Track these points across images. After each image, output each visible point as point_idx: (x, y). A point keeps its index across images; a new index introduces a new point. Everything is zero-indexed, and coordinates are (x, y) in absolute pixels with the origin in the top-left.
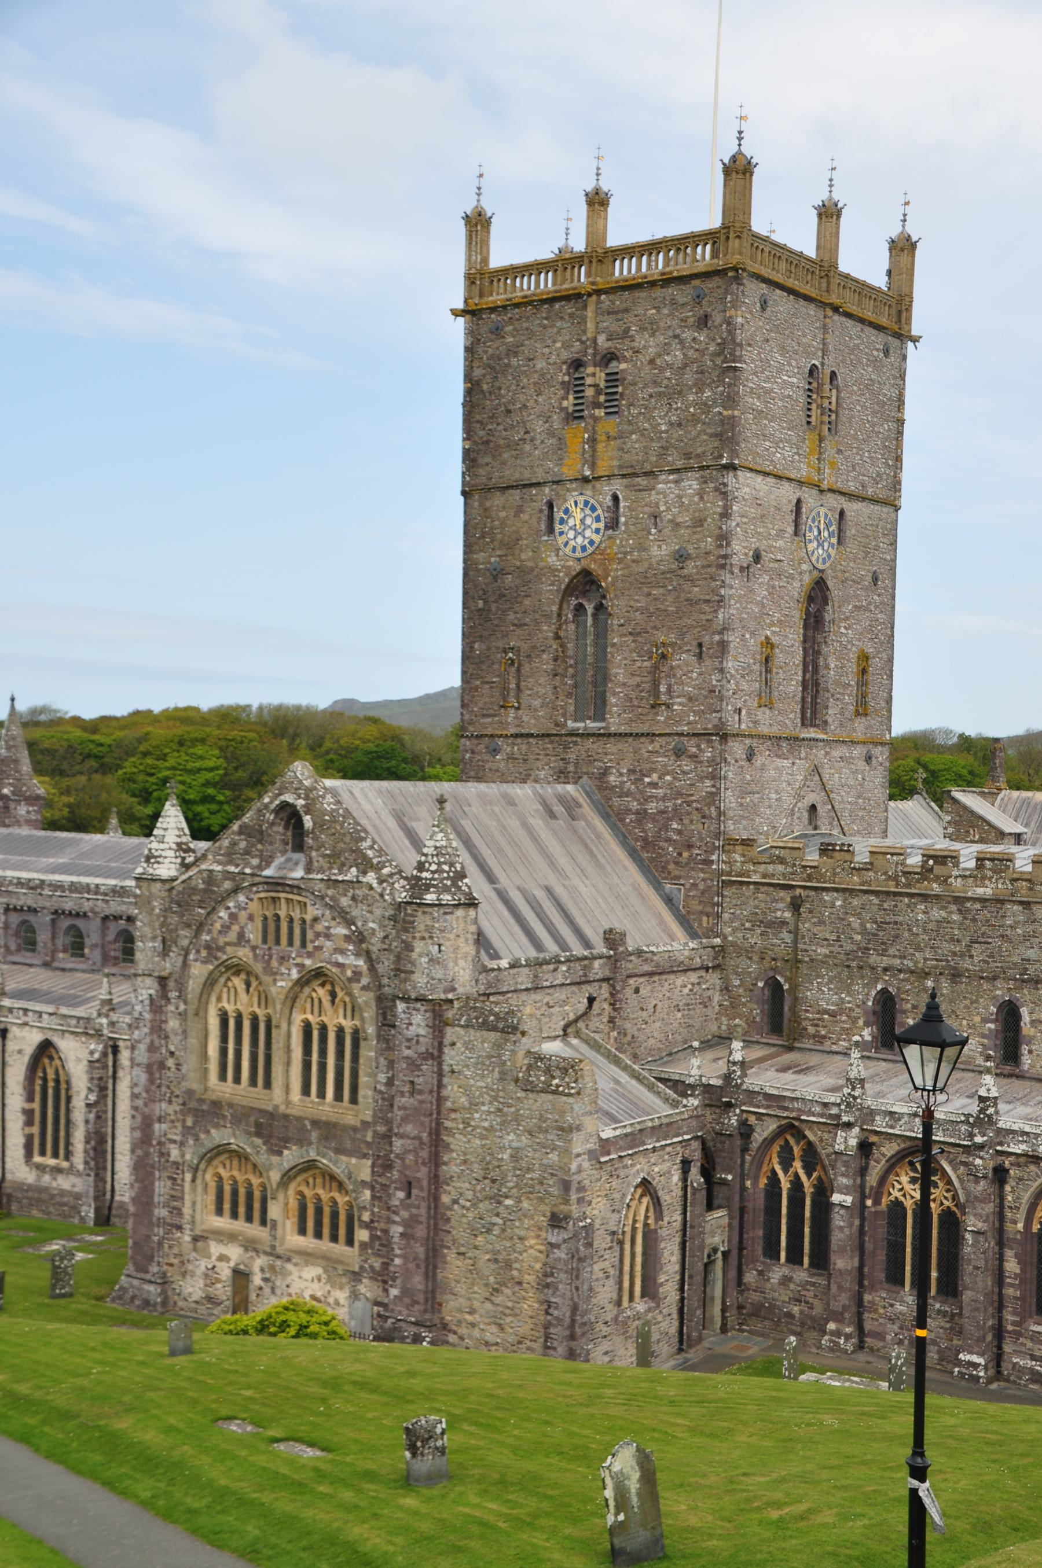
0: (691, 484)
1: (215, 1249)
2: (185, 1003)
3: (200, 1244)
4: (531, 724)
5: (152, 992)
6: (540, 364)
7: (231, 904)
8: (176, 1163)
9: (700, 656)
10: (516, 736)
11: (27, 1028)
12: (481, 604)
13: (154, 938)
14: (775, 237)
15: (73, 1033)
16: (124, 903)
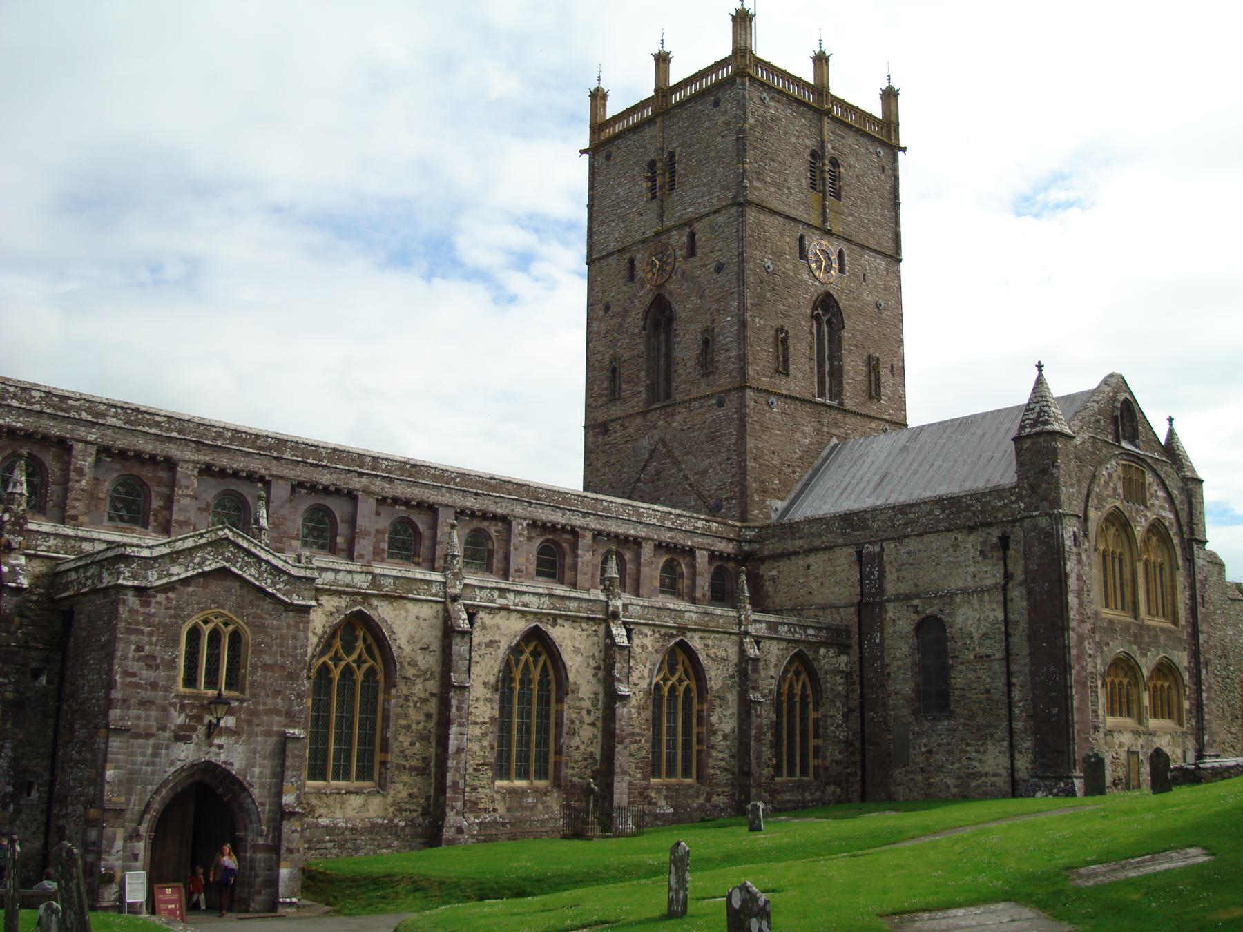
0: (882, 263)
1: (1118, 738)
2: (1089, 541)
3: (1108, 737)
4: (795, 390)
5: (1075, 529)
6: (793, 140)
7: (1109, 466)
8: (1092, 673)
9: (892, 371)
10: (786, 397)
11: (503, 613)
12: (759, 290)
13: (1072, 486)
15: (567, 618)
16: (417, 484)
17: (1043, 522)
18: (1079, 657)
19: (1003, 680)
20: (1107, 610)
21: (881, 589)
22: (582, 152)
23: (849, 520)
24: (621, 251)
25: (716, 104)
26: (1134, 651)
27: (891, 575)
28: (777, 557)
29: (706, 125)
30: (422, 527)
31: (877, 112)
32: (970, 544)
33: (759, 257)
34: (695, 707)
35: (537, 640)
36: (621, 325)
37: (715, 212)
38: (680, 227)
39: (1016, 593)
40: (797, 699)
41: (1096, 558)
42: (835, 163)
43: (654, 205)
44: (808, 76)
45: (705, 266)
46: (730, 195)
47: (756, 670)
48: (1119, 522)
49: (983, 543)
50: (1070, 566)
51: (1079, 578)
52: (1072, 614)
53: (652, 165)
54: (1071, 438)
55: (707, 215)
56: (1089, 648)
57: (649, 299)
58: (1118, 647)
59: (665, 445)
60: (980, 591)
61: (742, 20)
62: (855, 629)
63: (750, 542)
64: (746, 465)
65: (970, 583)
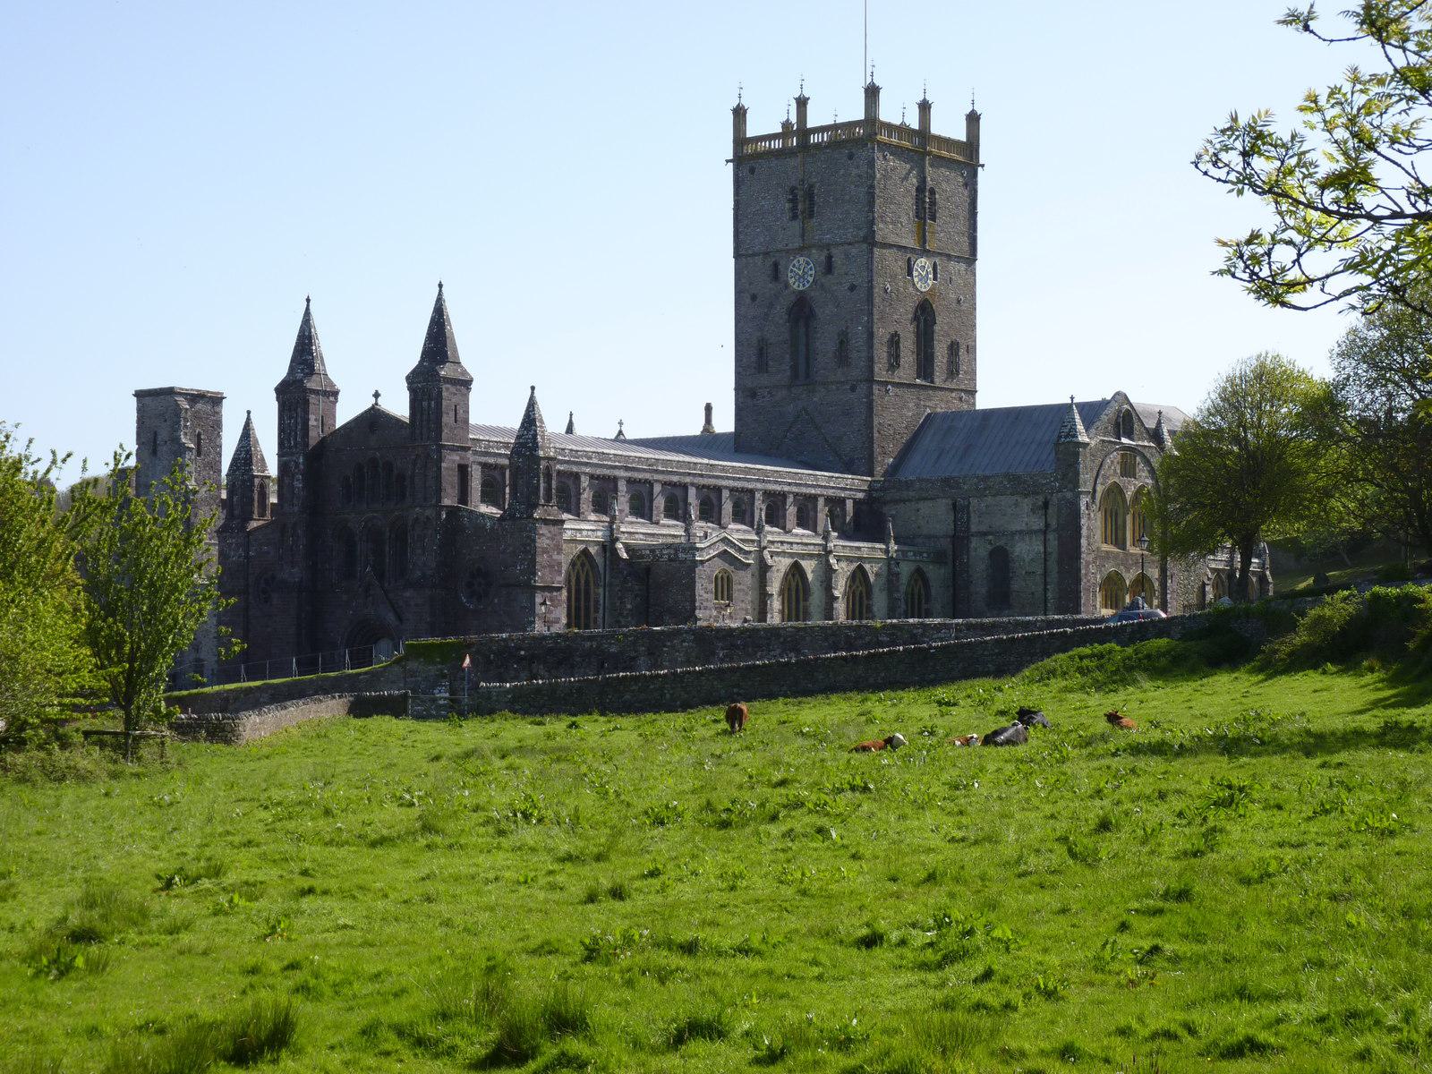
0: (963, 266)
14: (840, 120)
17: (1069, 495)
18: (1086, 574)
19: (1042, 587)
20: (1105, 545)
21: (968, 528)
22: (727, 161)
23: (947, 482)
24: (766, 254)
25: (851, 157)
26: (1122, 570)
27: (974, 519)
28: (896, 502)
29: (842, 172)
30: (715, 501)
31: (961, 136)
32: (1026, 504)
33: (880, 282)
34: (865, 602)
35: (796, 569)
36: (766, 314)
37: (850, 244)
38: (821, 247)
39: (1051, 536)
40: (916, 597)
41: (1100, 515)
42: (932, 192)
43: (796, 225)
44: (915, 125)
45: (841, 284)
46: (862, 234)
47: (898, 580)
48: (1115, 491)
49: (1034, 505)
50: (1083, 521)
51: (1088, 528)
52: (1083, 550)
53: (793, 190)
54: (1088, 444)
55: (842, 244)
56: (1092, 569)
57: (793, 298)
58: (1110, 568)
59: (807, 414)
60: (1031, 532)
61: (872, 93)
62: (950, 553)
63: (876, 491)
64: (873, 437)
65: (1024, 527)
